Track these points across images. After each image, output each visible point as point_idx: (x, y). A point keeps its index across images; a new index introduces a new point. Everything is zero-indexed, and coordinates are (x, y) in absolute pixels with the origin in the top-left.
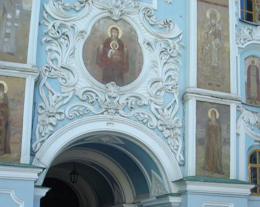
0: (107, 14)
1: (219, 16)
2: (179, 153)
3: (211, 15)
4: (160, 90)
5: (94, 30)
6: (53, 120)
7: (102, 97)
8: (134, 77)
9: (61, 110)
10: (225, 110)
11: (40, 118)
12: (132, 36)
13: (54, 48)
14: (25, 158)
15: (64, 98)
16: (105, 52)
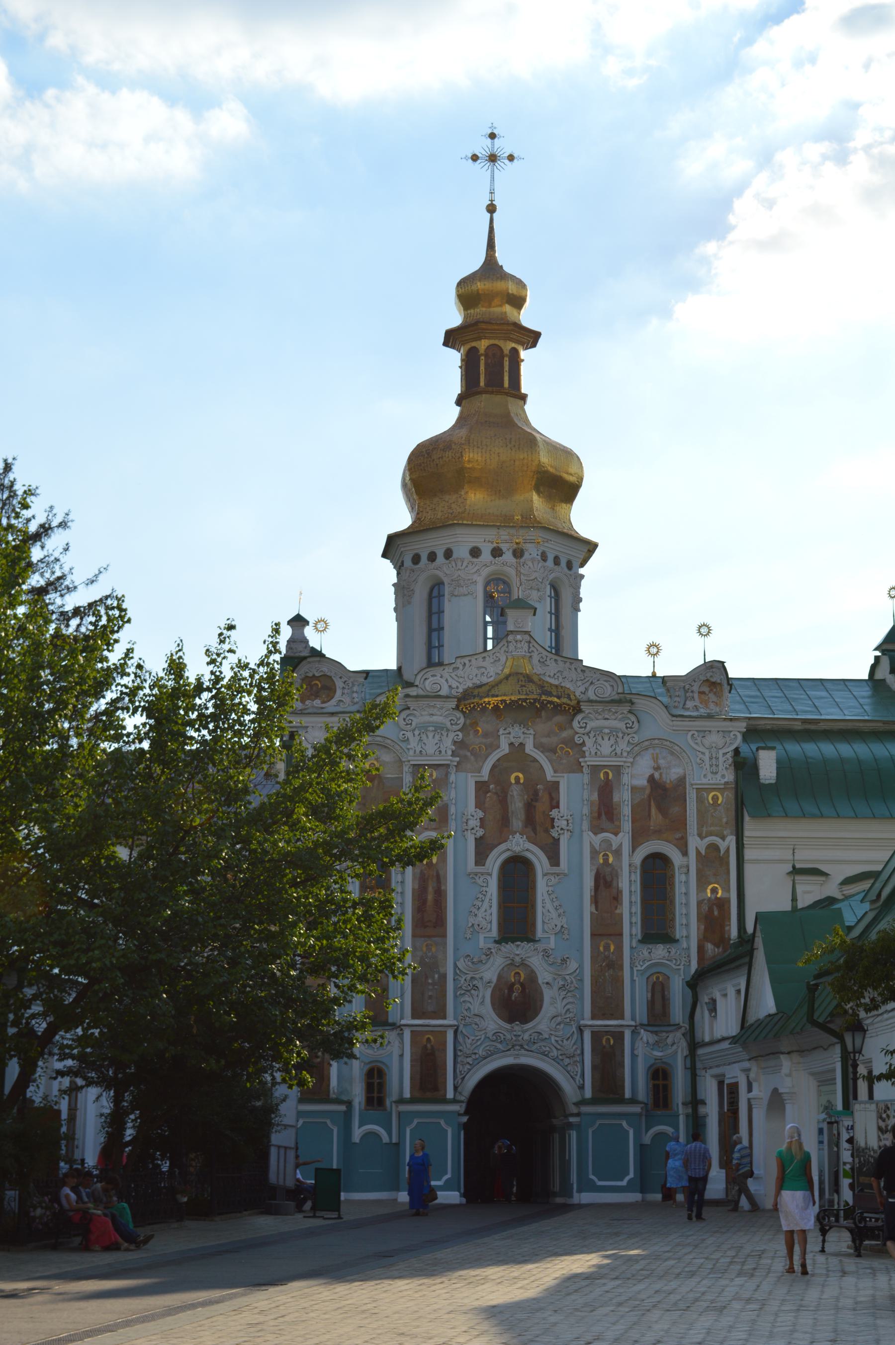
0: (509, 962)
1: (612, 948)
2: (578, 1078)
3: (604, 947)
4: (559, 1024)
5: (500, 977)
6: (469, 1060)
7: (508, 1036)
8: (536, 1012)
9: (476, 1051)
10: (619, 1037)
11: (459, 1059)
12: (532, 977)
13: (467, 999)
14: (450, 1094)
15: (478, 1040)
16: (510, 996)
